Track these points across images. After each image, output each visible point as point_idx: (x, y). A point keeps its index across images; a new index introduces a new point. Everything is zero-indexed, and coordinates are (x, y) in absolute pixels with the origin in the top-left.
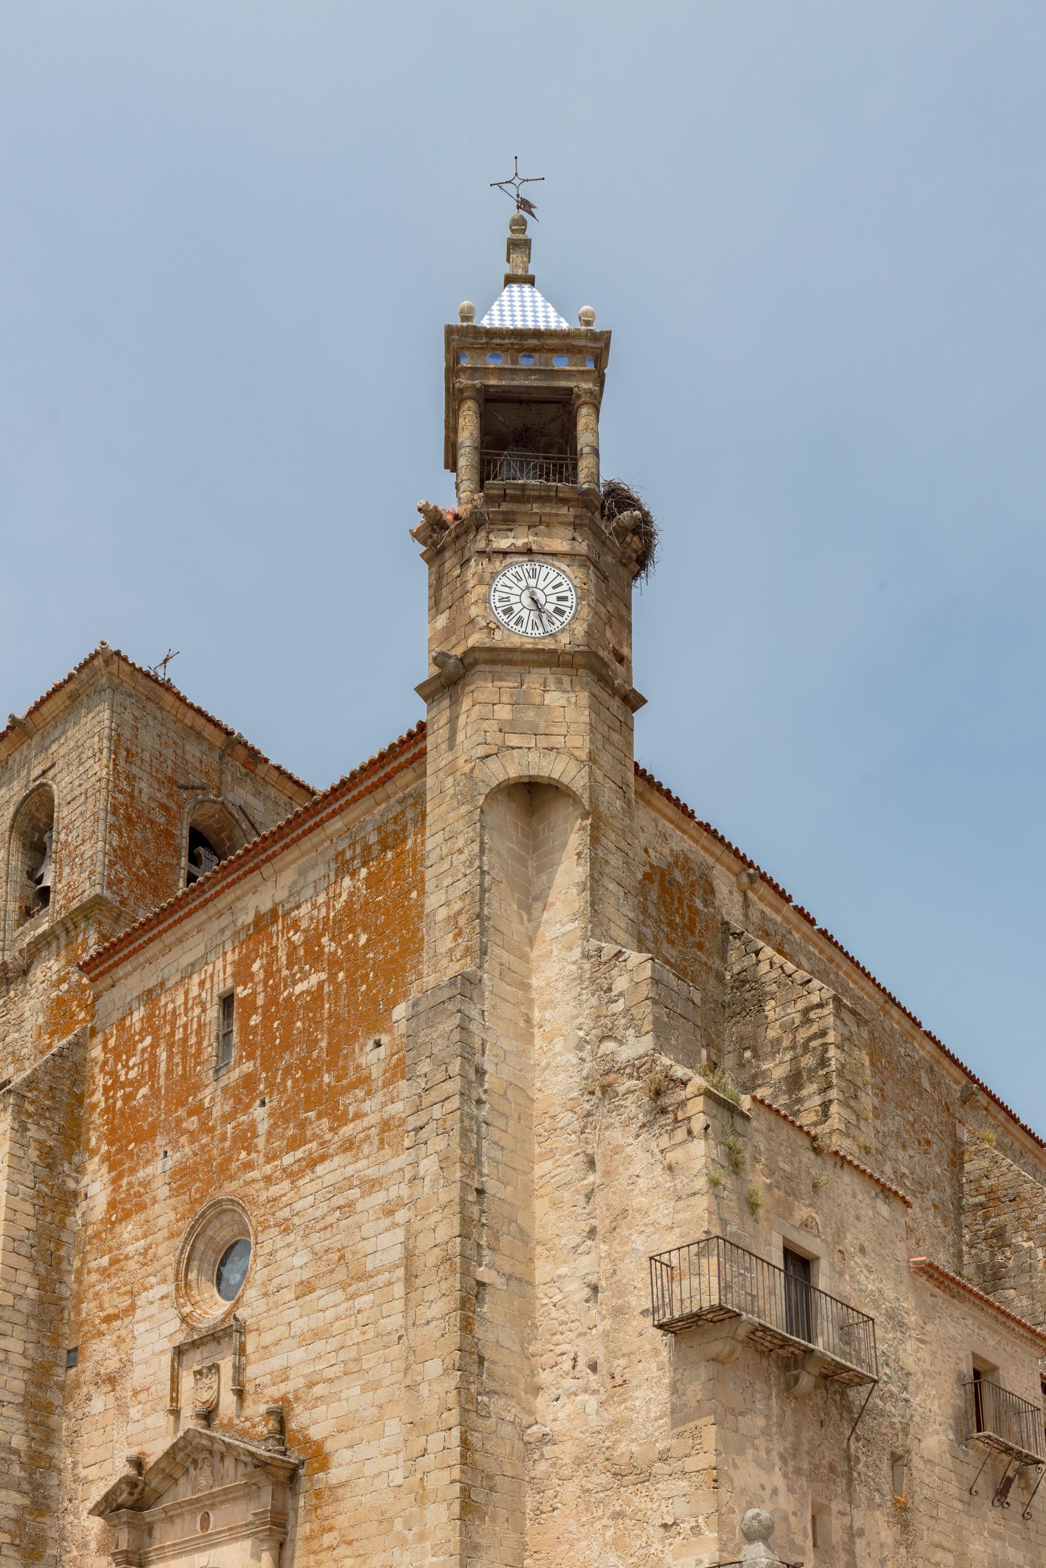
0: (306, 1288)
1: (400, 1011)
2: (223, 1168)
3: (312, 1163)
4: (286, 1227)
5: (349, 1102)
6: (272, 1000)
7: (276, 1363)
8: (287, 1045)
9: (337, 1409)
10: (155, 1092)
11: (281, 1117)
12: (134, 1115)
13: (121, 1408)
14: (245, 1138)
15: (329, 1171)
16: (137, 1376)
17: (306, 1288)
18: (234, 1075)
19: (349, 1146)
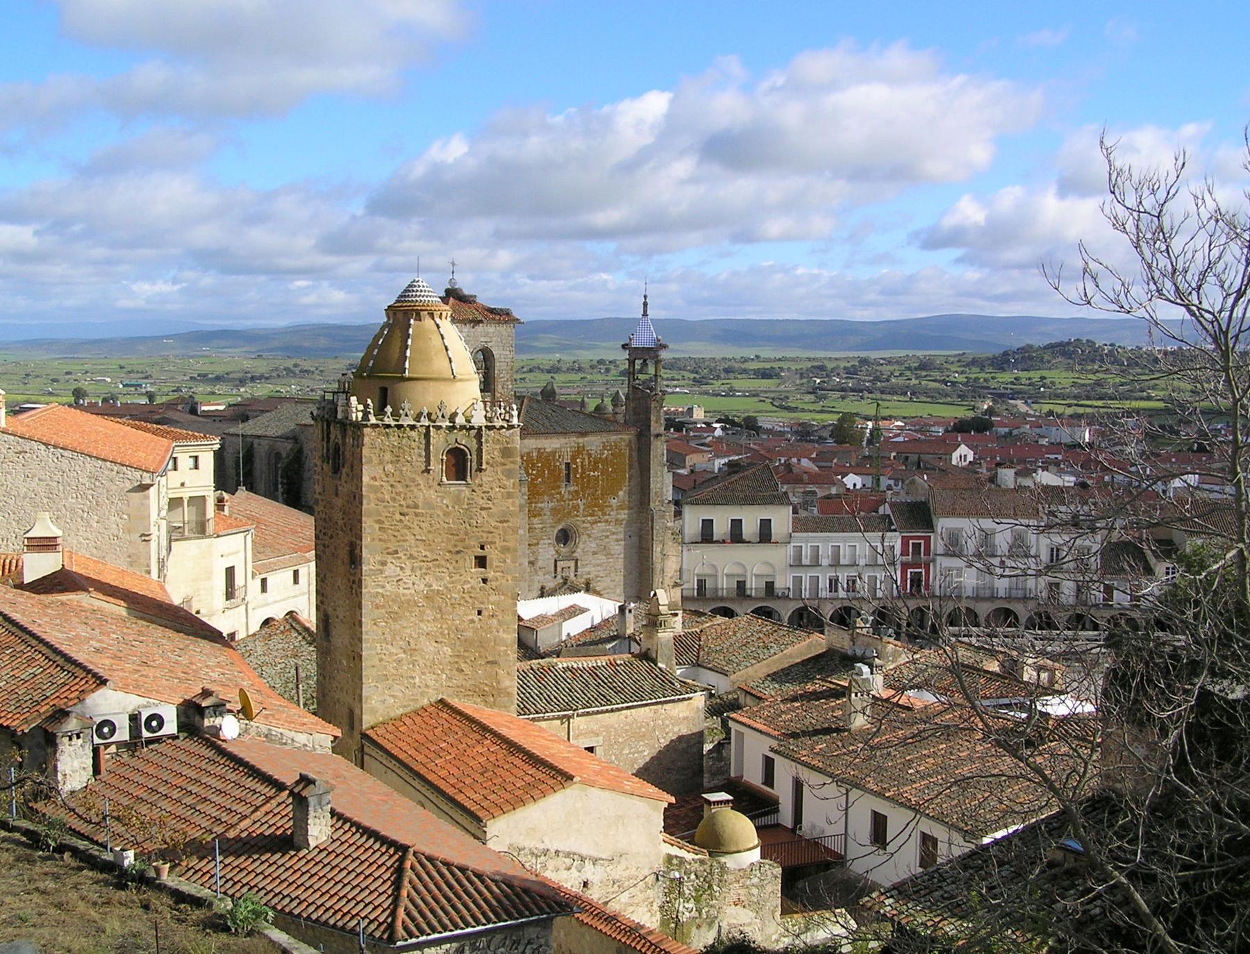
0: (594, 553)
1: (621, 493)
2: (569, 513)
3: (596, 522)
4: (589, 536)
5: (607, 510)
6: (583, 472)
7: (587, 569)
8: (588, 487)
9: (604, 585)
10: (543, 482)
11: (587, 506)
12: (535, 486)
13: (536, 572)
14: (576, 508)
15: (602, 525)
16: (540, 564)
17: (594, 553)
18: (572, 489)
19: (606, 521)
